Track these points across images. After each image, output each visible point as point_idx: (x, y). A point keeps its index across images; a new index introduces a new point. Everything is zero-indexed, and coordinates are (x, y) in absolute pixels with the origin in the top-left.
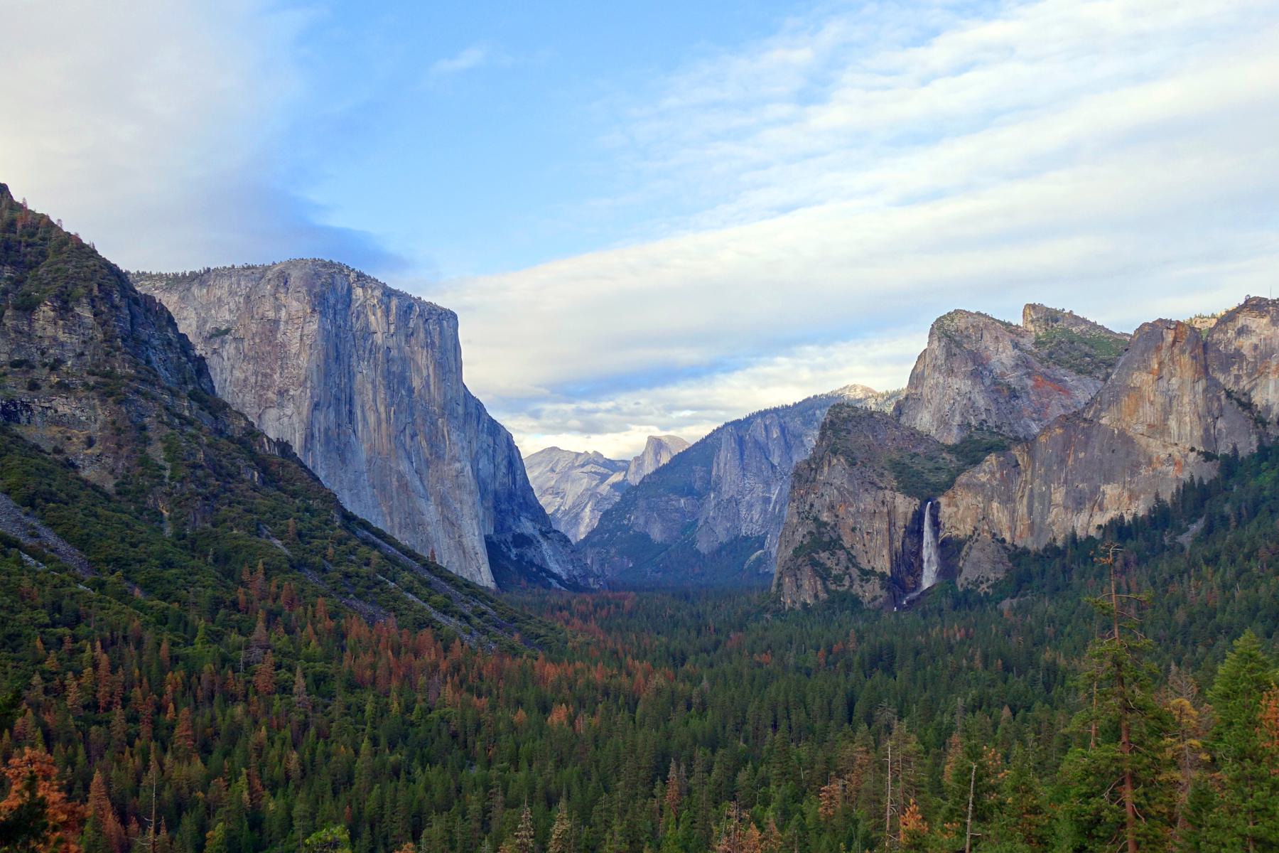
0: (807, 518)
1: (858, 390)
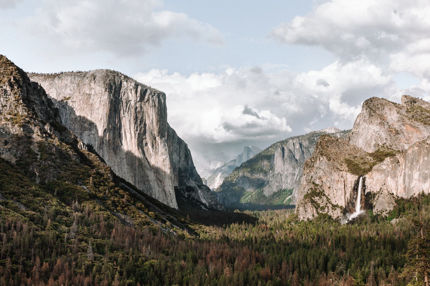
0: (310, 182)
1: (332, 129)
